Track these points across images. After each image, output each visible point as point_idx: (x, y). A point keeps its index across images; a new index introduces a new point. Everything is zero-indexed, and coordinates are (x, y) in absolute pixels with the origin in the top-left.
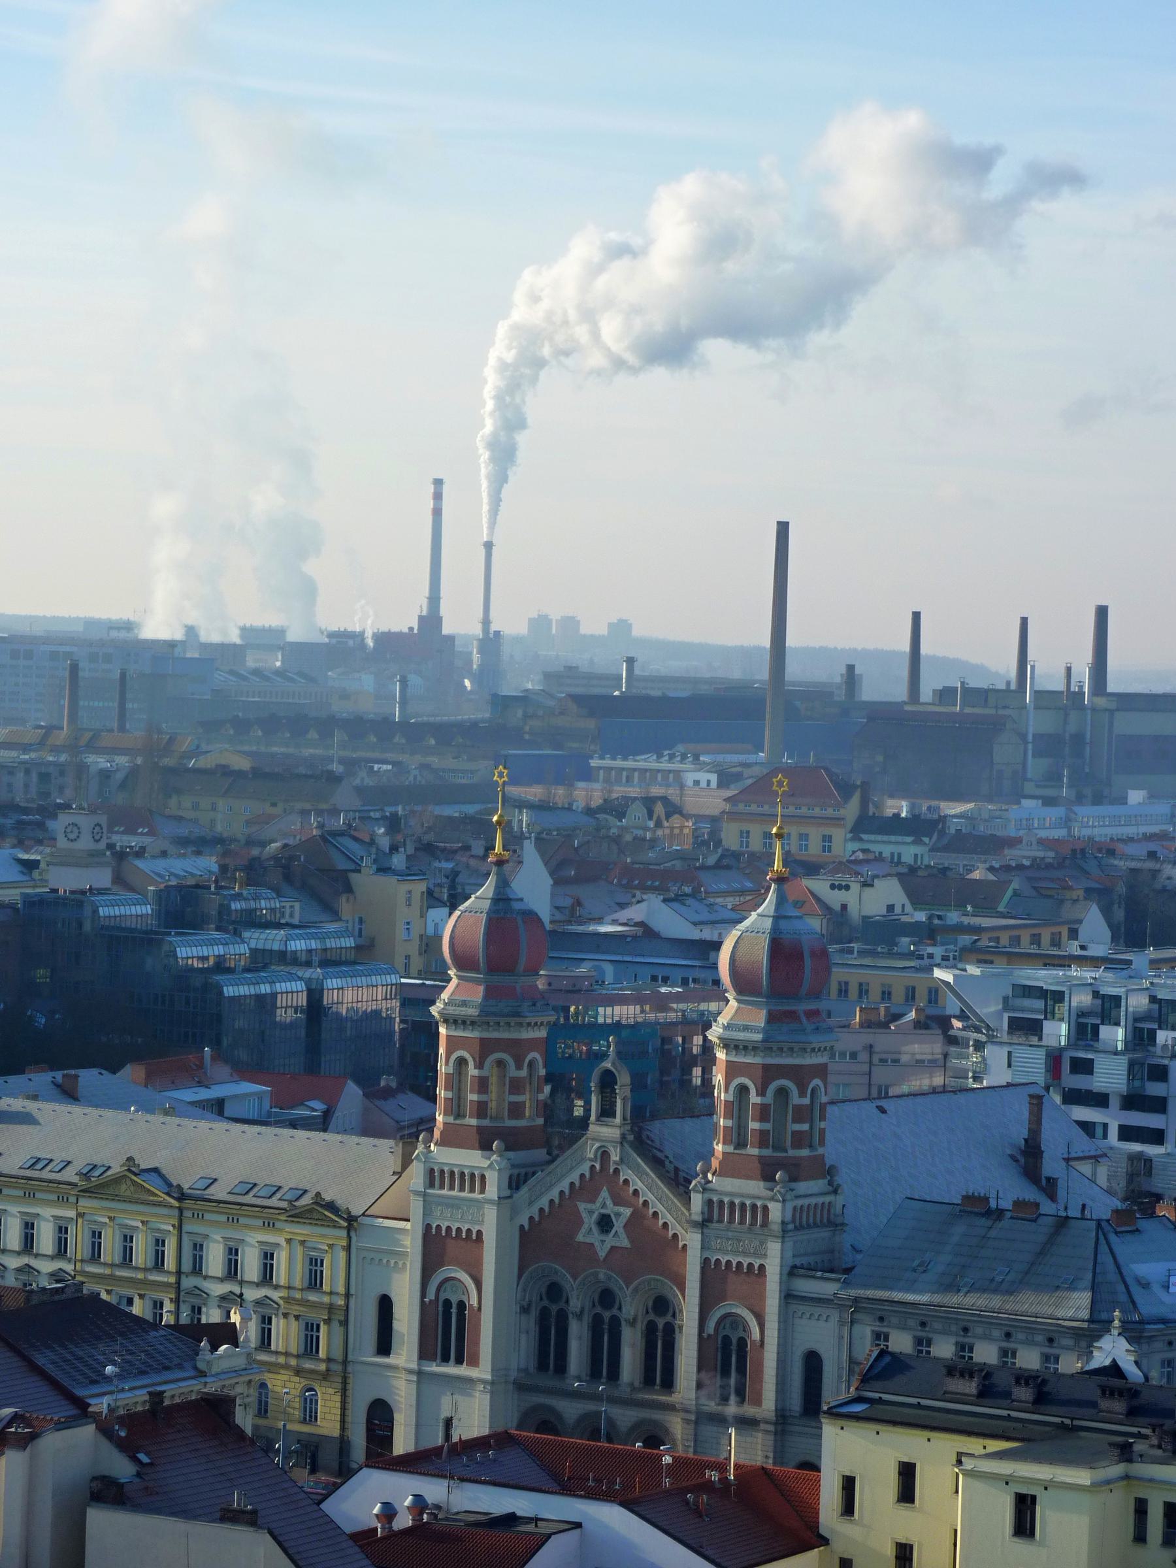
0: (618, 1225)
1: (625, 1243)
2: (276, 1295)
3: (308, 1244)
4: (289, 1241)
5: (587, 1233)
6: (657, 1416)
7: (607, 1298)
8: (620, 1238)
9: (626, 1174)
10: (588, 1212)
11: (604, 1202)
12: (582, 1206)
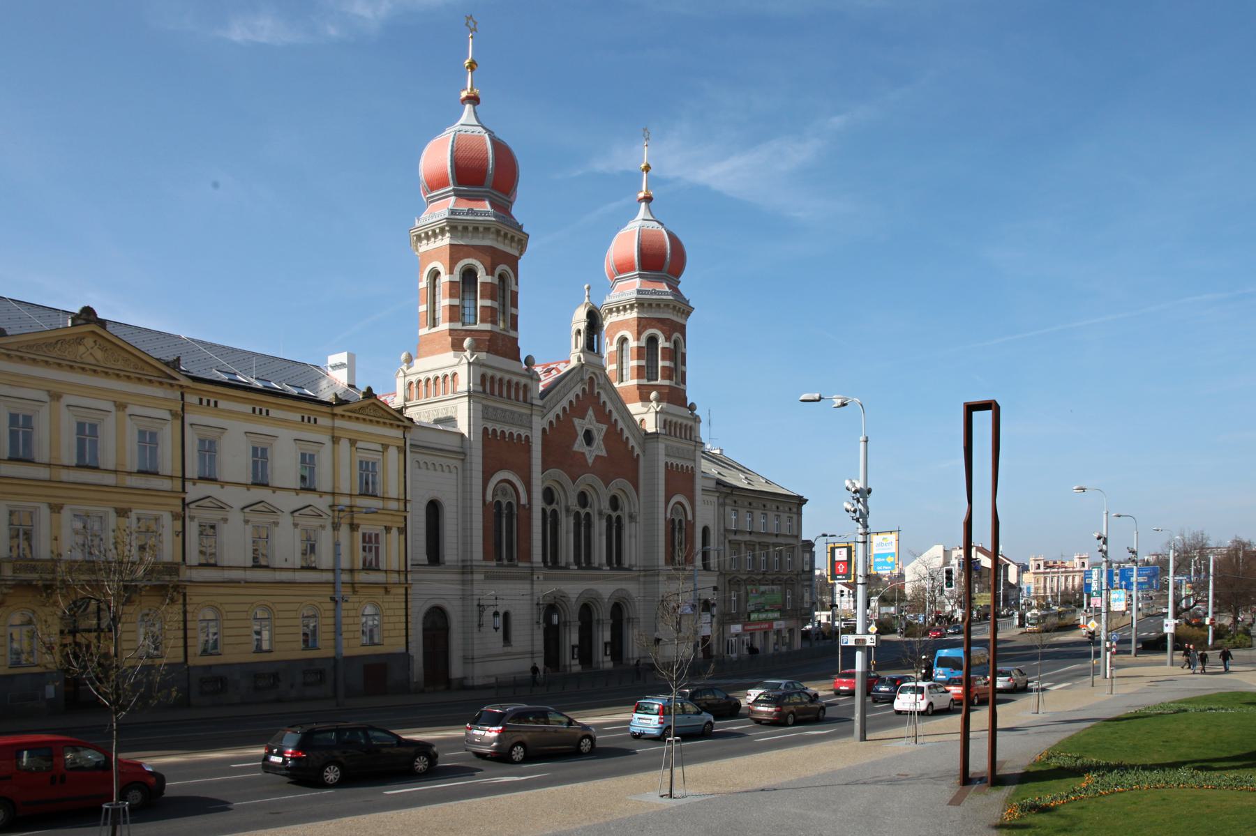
0: (598, 438)
1: (604, 453)
2: (322, 503)
3: (359, 444)
4: (335, 440)
5: (579, 445)
6: (624, 585)
7: (583, 499)
8: (599, 449)
9: (604, 397)
10: (581, 425)
11: (588, 421)
12: (577, 421)
